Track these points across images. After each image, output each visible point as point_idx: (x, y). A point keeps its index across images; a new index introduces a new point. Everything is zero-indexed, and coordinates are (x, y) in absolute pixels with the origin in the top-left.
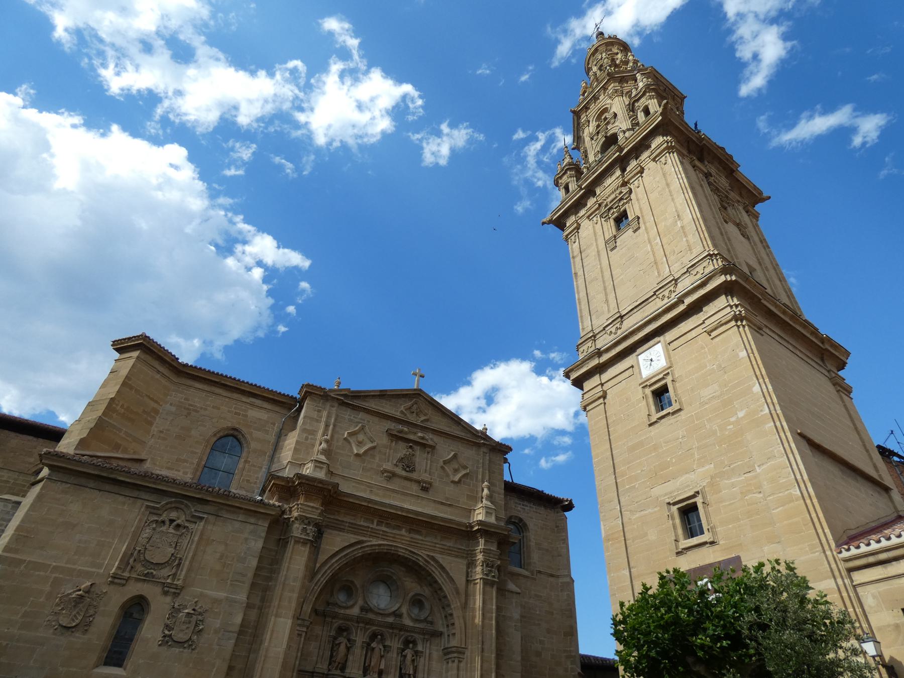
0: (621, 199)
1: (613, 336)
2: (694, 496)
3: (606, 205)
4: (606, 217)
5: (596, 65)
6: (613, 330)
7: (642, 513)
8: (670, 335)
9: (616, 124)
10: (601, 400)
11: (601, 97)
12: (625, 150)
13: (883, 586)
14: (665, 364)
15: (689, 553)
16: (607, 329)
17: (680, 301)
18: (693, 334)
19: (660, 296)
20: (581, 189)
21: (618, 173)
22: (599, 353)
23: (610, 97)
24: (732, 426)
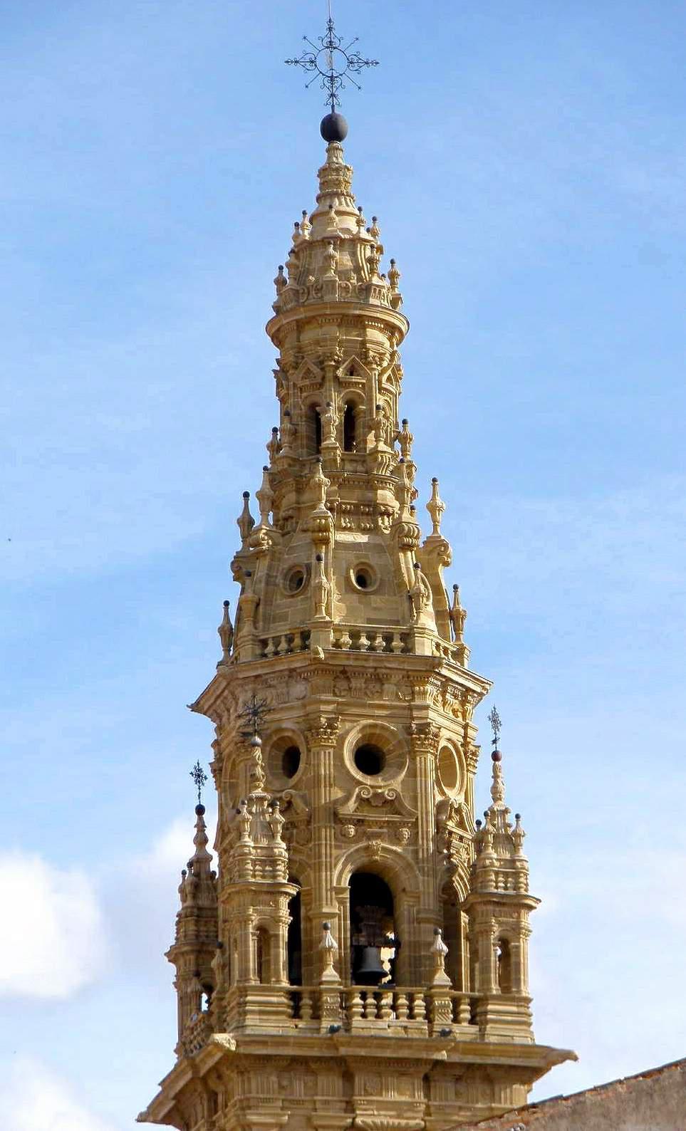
21: (418, 1082)
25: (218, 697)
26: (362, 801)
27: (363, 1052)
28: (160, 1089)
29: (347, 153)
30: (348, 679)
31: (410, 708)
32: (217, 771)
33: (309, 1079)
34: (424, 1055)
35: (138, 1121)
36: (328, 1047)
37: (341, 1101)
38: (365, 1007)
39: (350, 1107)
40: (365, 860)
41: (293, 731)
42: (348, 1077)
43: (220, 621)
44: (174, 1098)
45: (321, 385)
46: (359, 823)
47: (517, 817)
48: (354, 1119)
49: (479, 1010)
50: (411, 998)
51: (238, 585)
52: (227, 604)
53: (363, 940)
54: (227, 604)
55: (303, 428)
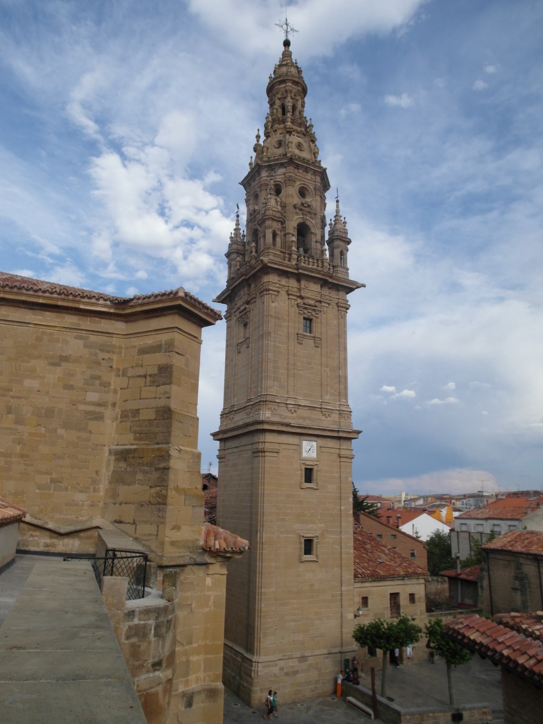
0: (314, 310)
1: (290, 414)
3: (304, 304)
4: (301, 310)
5: (292, 98)
6: (293, 410)
7: (287, 535)
8: (322, 442)
9: (313, 222)
10: (276, 455)
13: (360, 589)
14: (316, 457)
15: (306, 563)
16: (289, 406)
17: (338, 431)
18: (333, 451)
20: (297, 269)
21: (319, 287)
22: (288, 425)
23: (315, 189)
24: (336, 511)
26: (302, 204)
27: (306, 273)
29: (291, 48)
30: (298, 169)
32: (247, 201)
33: (287, 280)
36: (296, 269)
38: (305, 260)
39: (299, 289)
40: (302, 221)
41: (280, 182)
42: (299, 281)
43: (249, 161)
45: (286, 98)
46: (301, 210)
47: (345, 218)
49: (335, 269)
50: (317, 260)
51: (255, 154)
52: (252, 157)
54: (252, 157)
55: (280, 110)
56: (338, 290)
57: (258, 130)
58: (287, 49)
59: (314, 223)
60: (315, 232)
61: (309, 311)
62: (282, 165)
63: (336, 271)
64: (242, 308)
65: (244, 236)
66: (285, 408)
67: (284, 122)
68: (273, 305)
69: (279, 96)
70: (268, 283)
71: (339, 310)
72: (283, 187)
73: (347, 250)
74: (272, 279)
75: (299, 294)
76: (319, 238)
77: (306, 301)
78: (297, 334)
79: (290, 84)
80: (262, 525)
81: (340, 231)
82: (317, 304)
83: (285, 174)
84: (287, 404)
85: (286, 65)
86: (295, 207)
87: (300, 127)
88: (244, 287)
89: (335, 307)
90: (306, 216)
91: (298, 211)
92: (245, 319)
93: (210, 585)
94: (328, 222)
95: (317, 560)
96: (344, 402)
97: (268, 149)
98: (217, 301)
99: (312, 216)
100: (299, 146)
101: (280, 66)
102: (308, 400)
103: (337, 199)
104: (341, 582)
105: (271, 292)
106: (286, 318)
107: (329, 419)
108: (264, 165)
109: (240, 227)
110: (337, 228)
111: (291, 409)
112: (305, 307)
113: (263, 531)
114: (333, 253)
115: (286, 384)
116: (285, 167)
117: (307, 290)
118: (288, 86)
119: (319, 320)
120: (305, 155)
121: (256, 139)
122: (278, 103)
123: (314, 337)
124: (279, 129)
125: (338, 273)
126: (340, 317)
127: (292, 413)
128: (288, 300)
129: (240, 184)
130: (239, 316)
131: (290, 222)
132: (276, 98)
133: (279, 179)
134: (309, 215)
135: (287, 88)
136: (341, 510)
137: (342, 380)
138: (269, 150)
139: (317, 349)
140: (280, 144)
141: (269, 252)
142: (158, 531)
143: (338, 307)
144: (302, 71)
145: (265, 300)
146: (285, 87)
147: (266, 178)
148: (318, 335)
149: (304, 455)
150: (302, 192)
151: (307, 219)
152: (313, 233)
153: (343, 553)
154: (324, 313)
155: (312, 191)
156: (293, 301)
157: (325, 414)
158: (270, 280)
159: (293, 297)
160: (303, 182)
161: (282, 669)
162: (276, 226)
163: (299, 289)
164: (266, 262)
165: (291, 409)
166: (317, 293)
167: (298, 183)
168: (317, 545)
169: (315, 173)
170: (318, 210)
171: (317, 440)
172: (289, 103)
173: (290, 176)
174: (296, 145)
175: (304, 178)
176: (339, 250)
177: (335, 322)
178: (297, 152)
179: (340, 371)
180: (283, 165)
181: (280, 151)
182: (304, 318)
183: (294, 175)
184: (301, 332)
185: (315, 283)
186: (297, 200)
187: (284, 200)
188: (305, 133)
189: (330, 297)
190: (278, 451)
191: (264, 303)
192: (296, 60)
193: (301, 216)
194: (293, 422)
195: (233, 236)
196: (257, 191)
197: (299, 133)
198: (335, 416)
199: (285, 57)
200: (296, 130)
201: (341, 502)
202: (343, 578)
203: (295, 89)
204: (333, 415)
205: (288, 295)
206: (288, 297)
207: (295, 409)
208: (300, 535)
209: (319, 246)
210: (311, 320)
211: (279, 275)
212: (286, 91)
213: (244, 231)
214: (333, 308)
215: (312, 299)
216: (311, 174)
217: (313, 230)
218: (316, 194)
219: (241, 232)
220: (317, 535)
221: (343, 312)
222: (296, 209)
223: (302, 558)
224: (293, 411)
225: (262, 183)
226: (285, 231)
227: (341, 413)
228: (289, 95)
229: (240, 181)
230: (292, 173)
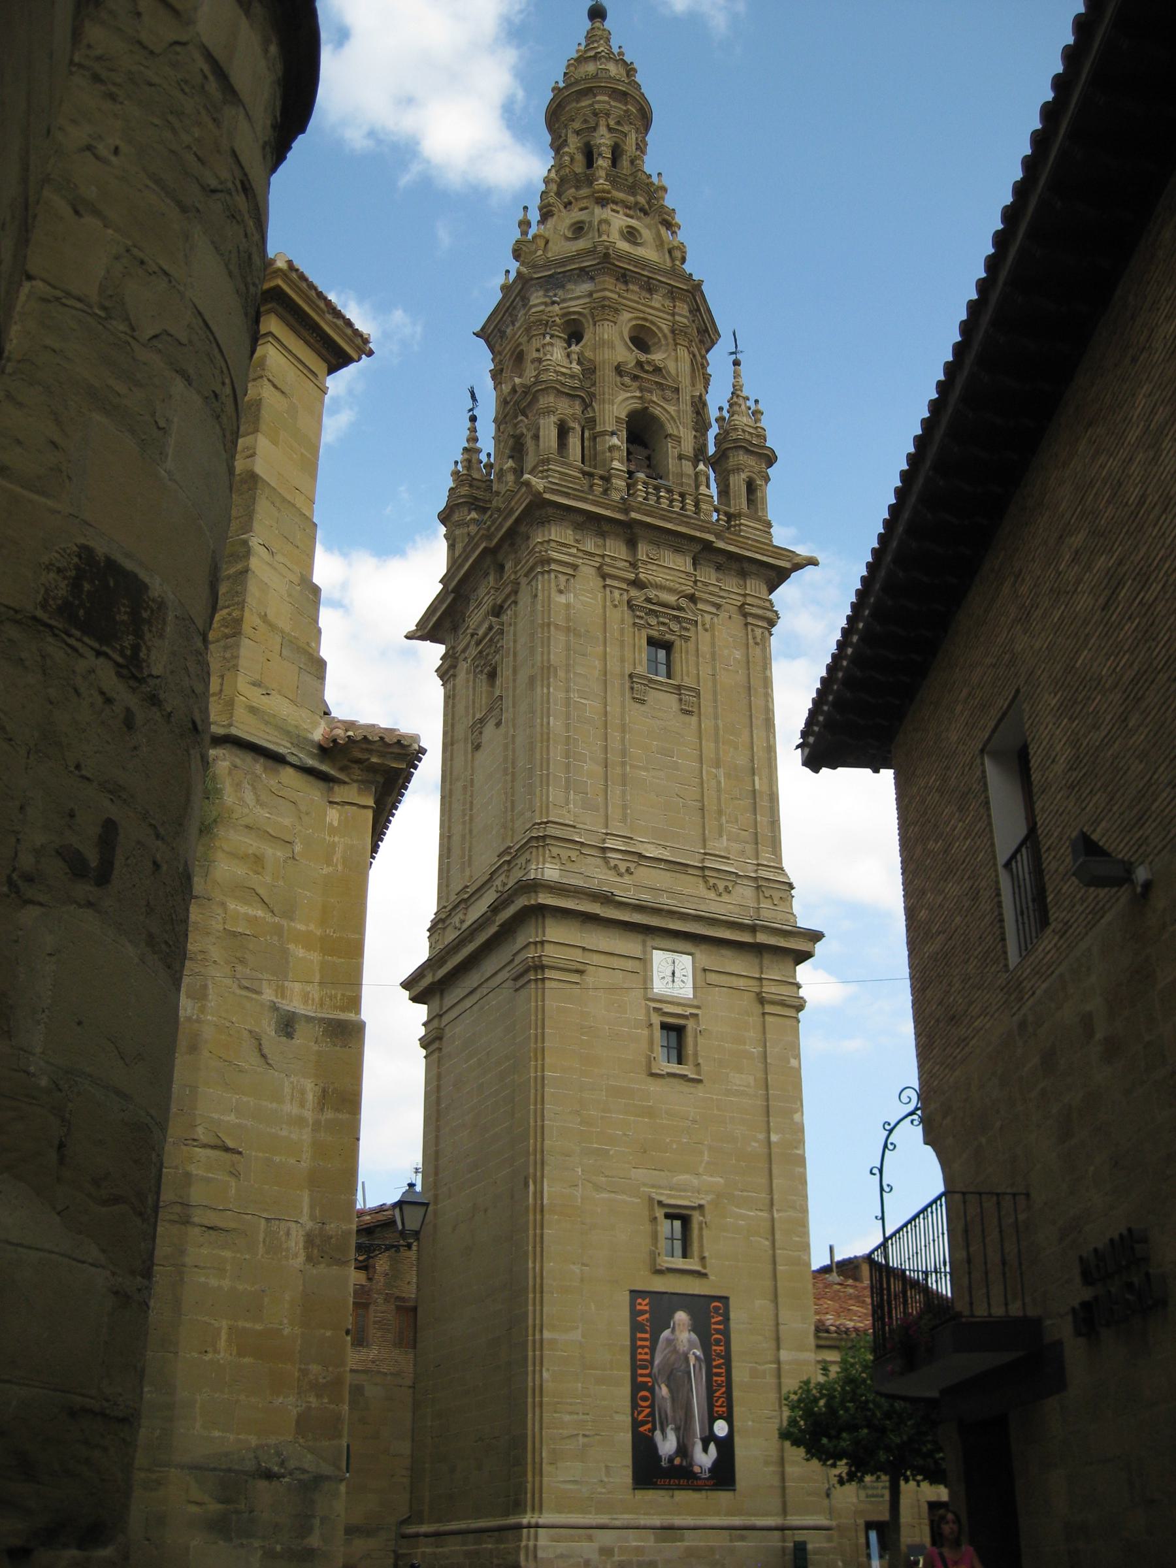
1: (612, 877)
2: (693, 1208)
3: (648, 600)
5: (610, 129)
7: (613, 1195)
9: (671, 409)
10: (575, 978)
11: (657, 300)
12: (721, 545)
17: (753, 929)
18: (741, 983)
19: (712, 881)
20: (626, 511)
21: (689, 561)
22: (607, 899)
23: (673, 332)
25: (508, 308)
26: (639, 364)
27: (649, 520)
28: (441, 586)
29: (608, 24)
30: (626, 283)
31: (673, 315)
32: (496, 375)
33: (600, 541)
34: (698, 534)
35: (407, 637)
36: (620, 511)
37: (626, 561)
38: (647, 493)
39: (633, 565)
40: (638, 405)
42: (632, 544)
44: (452, 592)
45: (595, 129)
46: (635, 378)
47: (757, 401)
48: (637, 574)
50: (682, 495)
52: (508, 272)
53: (632, 468)
54: (508, 272)
55: (579, 157)
56: (743, 574)
57: (526, 208)
58: (598, 24)
59: (672, 413)
60: (676, 433)
61: (661, 619)
62: (584, 274)
63: (735, 526)
64: (481, 632)
65: (489, 466)
66: (599, 861)
67: (590, 181)
68: (562, 599)
69: (577, 125)
70: (545, 545)
71: (746, 624)
72: (586, 325)
73: (767, 479)
74: (559, 533)
75: (632, 576)
76: (688, 447)
77: (652, 593)
78: (631, 676)
79: (606, 98)
80: (539, 1161)
81: (744, 431)
82: (683, 603)
83: (590, 294)
84: (604, 849)
85: (595, 58)
86: (619, 370)
87: (634, 194)
88: (487, 574)
89: (737, 617)
90: (650, 392)
91: (627, 380)
92: (490, 657)
93: (336, 824)
94: (713, 413)
95: (704, 1271)
96: (770, 860)
97: (547, 242)
98: (419, 634)
99: (668, 393)
100: (631, 235)
101: (580, 60)
102: (665, 847)
103: (733, 357)
104: (778, 1340)
105: (553, 566)
106: (600, 635)
107: (725, 898)
108: (536, 276)
109: (479, 445)
110: (737, 422)
111: (616, 862)
112: (651, 610)
113: (542, 1177)
114: (728, 486)
115: (600, 799)
116: (592, 278)
117: (654, 568)
118: (599, 102)
119: (691, 645)
120: (648, 253)
121: (518, 231)
122: (574, 144)
123: (679, 687)
124: (576, 199)
125: (740, 531)
126: (751, 641)
127: (621, 875)
128: (602, 590)
129: (477, 334)
130: (474, 653)
131: (607, 406)
132: (570, 131)
133: (575, 306)
134: (660, 393)
135: (596, 106)
136: (769, 1143)
137: (763, 803)
138: (550, 244)
139: (687, 718)
140: (579, 229)
141: (547, 470)
142: (222, 684)
143: (745, 615)
144: (635, 71)
145: (540, 587)
146: (592, 105)
147: (542, 308)
148: (688, 682)
149: (660, 986)
150: (641, 340)
151: (654, 402)
152: (670, 435)
153: (778, 1260)
154: (706, 630)
155: (665, 336)
156: (617, 593)
157: (714, 886)
158: (553, 537)
159: (615, 583)
160: (642, 315)
161: (606, 1552)
162: (567, 409)
163: (633, 565)
164: (541, 490)
165: (616, 862)
166: (683, 576)
167: (626, 316)
168: (701, 1229)
169: (673, 294)
170: (685, 381)
171: (693, 951)
172: (603, 140)
173: (604, 298)
174: (621, 233)
175: (643, 304)
176: (743, 476)
177: (738, 654)
178: (623, 246)
179: (757, 778)
180: (587, 273)
181: (582, 244)
182: (651, 642)
183: (615, 296)
184: (641, 669)
185: (677, 550)
186: (625, 355)
187: (588, 354)
188: (647, 207)
189: (721, 589)
190: (581, 967)
191: (536, 596)
192: (620, 47)
193: (638, 394)
194: (621, 894)
195: (460, 467)
196: (520, 344)
197: (629, 208)
198: (744, 894)
199: (593, 42)
200: (623, 202)
201: (768, 1122)
202: (781, 1327)
203: (618, 108)
204: (739, 890)
205: (604, 576)
206: (602, 584)
207: (629, 864)
208: (651, 1199)
209: (687, 466)
210: (668, 646)
211: (578, 527)
212: (595, 114)
213: (489, 455)
214: (730, 617)
215: (671, 590)
216: (663, 296)
217: (670, 429)
218: (676, 344)
219: (483, 457)
220: (702, 1202)
221: (760, 630)
222: (621, 376)
223: (659, 1260)
224: (623, 870)
225: (532, 319)
226: (594, 429)
227: (759, 885)
228: (602, 122)
229: (478, 329)
230: (611, 291)
